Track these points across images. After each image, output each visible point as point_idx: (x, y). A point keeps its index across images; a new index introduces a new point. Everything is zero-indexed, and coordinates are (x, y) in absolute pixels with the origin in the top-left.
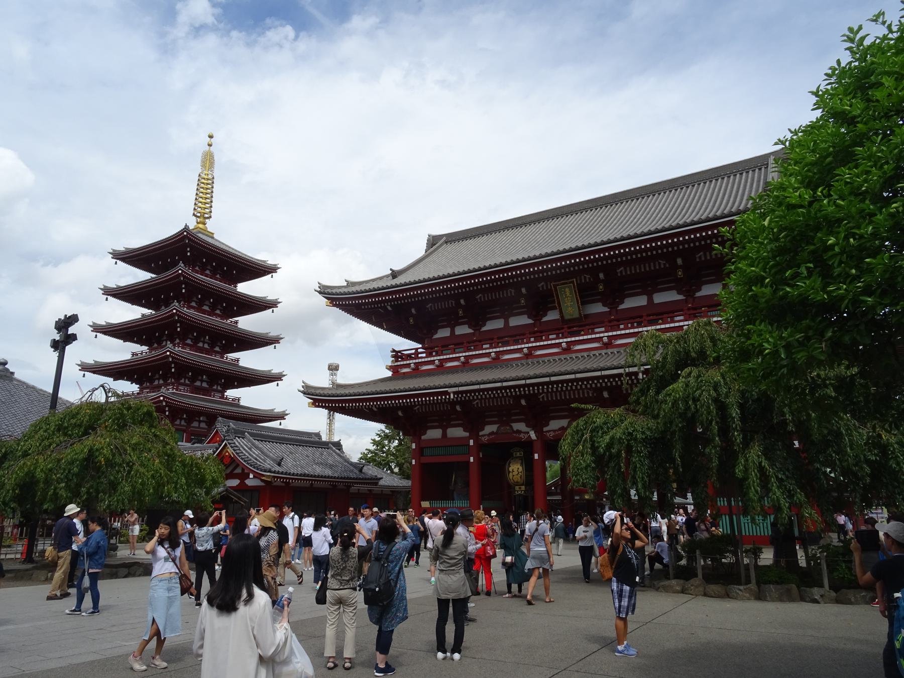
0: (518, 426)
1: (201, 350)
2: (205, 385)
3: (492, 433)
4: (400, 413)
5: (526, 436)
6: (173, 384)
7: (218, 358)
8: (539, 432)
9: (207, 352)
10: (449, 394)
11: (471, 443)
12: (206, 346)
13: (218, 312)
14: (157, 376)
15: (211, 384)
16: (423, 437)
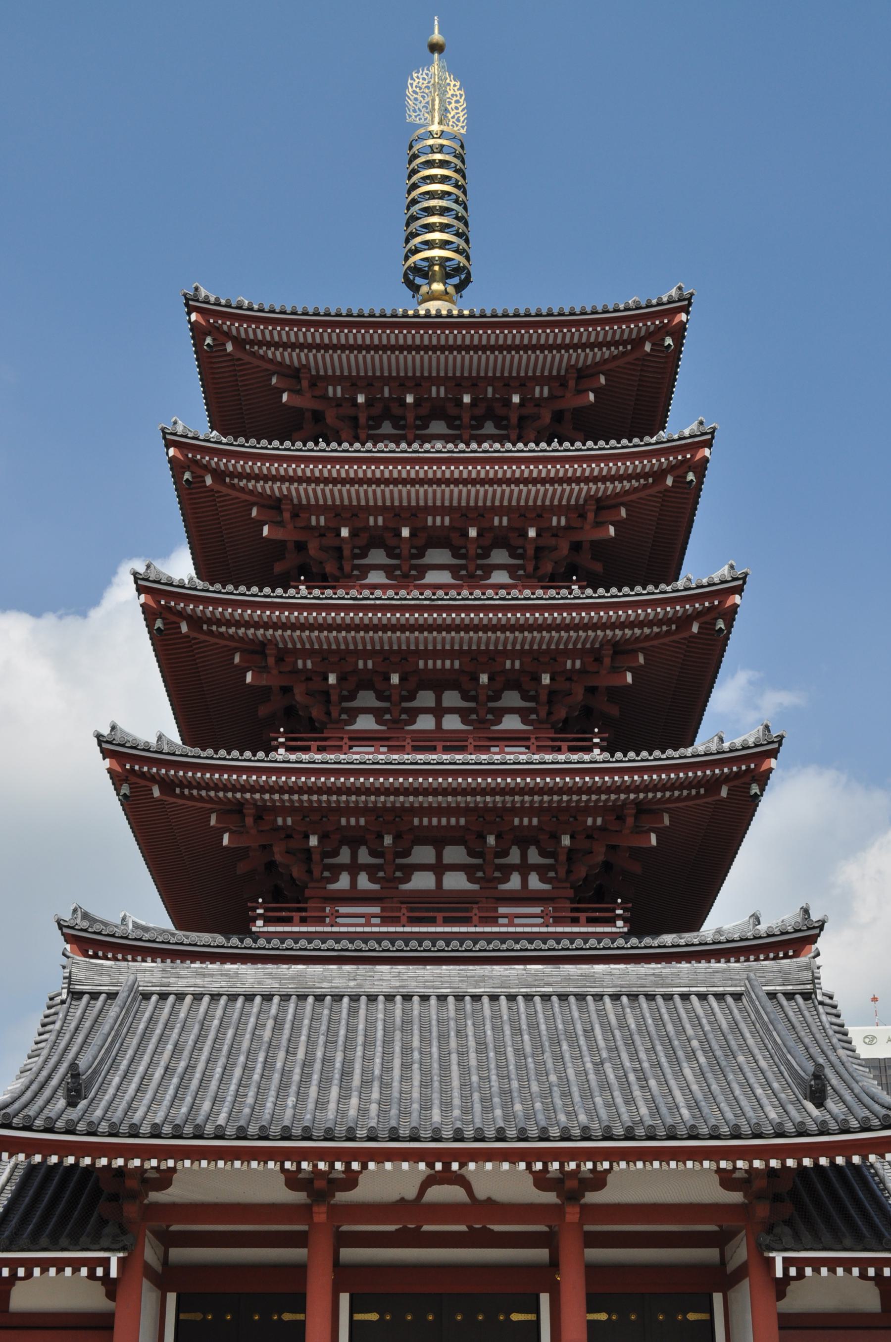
7: (518, 756)
12: (452, 722)
15: (487, 871)
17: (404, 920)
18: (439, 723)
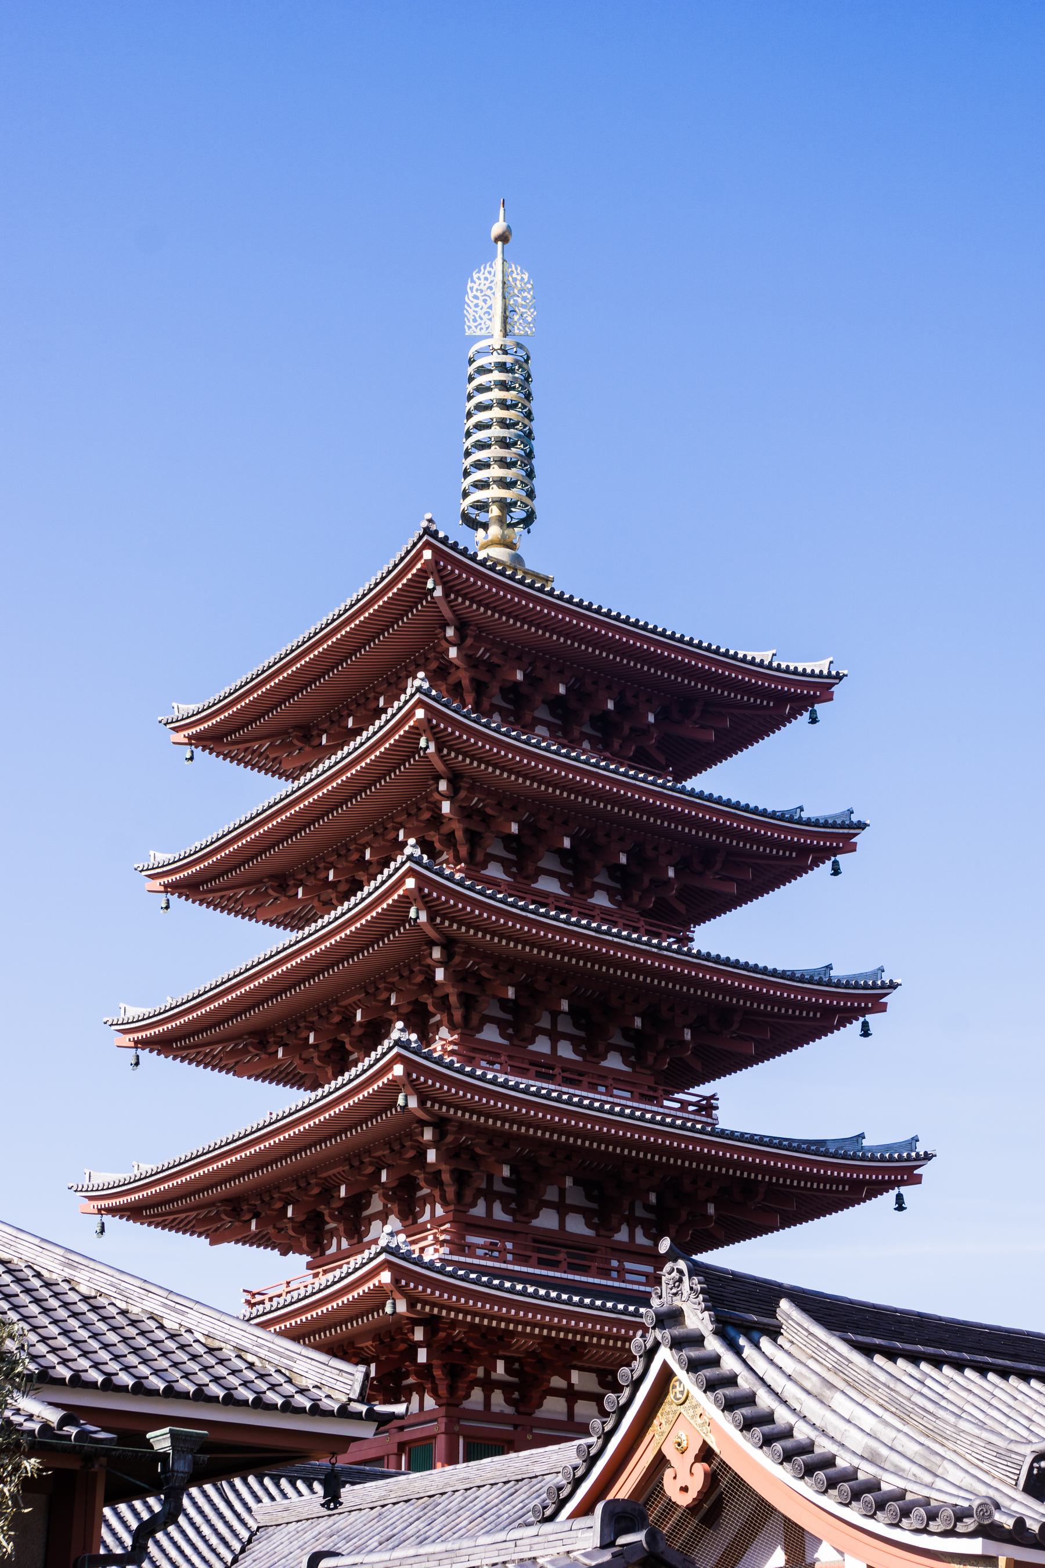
1: (543, 1069)
2: (576, 1225)
6: (437, 1222)
9: (572, 1077)
12: (566, 1051)
13: (601, 899)
14: (377, 1204)
15: (602, 1218)
17: (564, 1265)
18: (554, 1049)
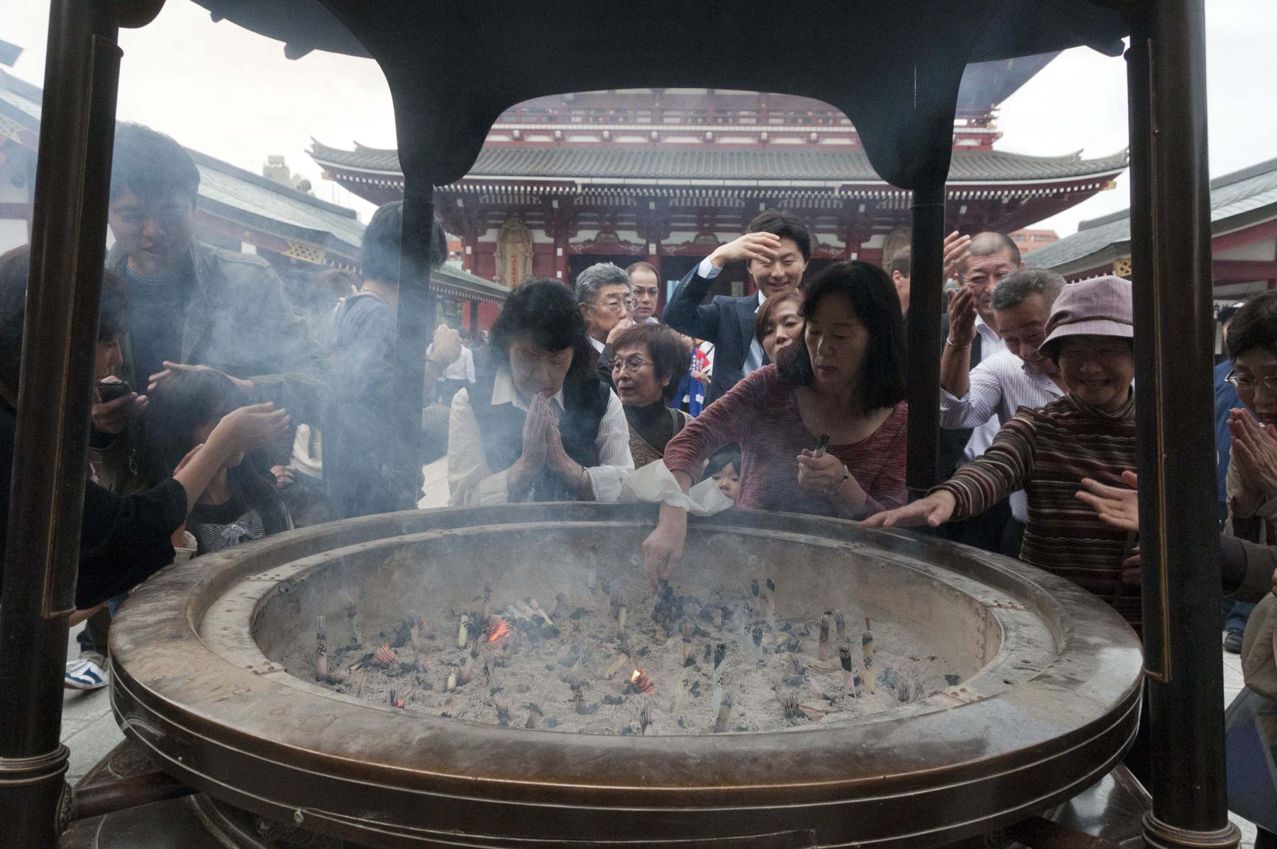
0: (623, 235)
3: (589, 241)
4: (460, 203)
5: (638, 249)
8: (659, 247)
10: (576, 186)
11: (560, 252)
16: (481, 239)
